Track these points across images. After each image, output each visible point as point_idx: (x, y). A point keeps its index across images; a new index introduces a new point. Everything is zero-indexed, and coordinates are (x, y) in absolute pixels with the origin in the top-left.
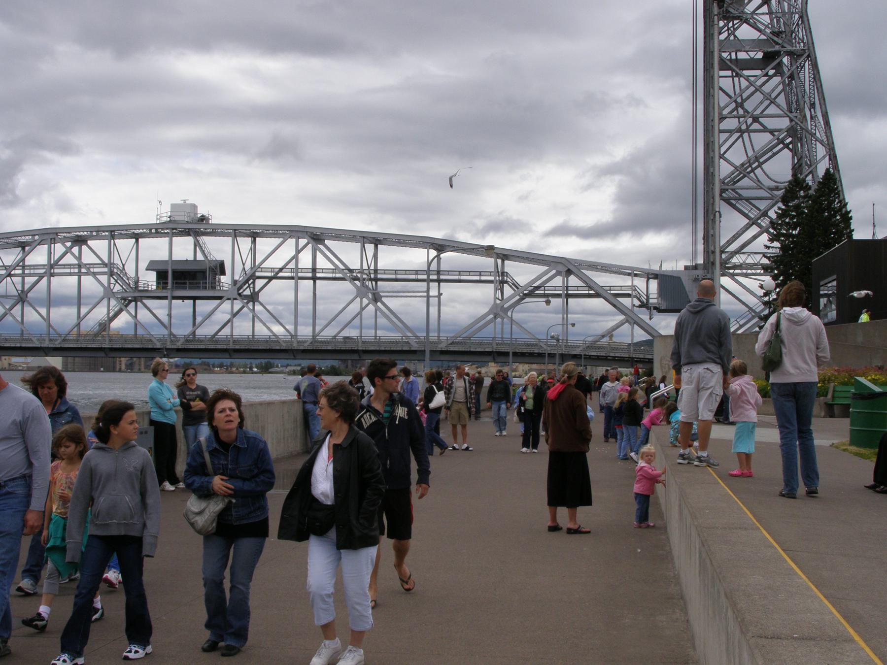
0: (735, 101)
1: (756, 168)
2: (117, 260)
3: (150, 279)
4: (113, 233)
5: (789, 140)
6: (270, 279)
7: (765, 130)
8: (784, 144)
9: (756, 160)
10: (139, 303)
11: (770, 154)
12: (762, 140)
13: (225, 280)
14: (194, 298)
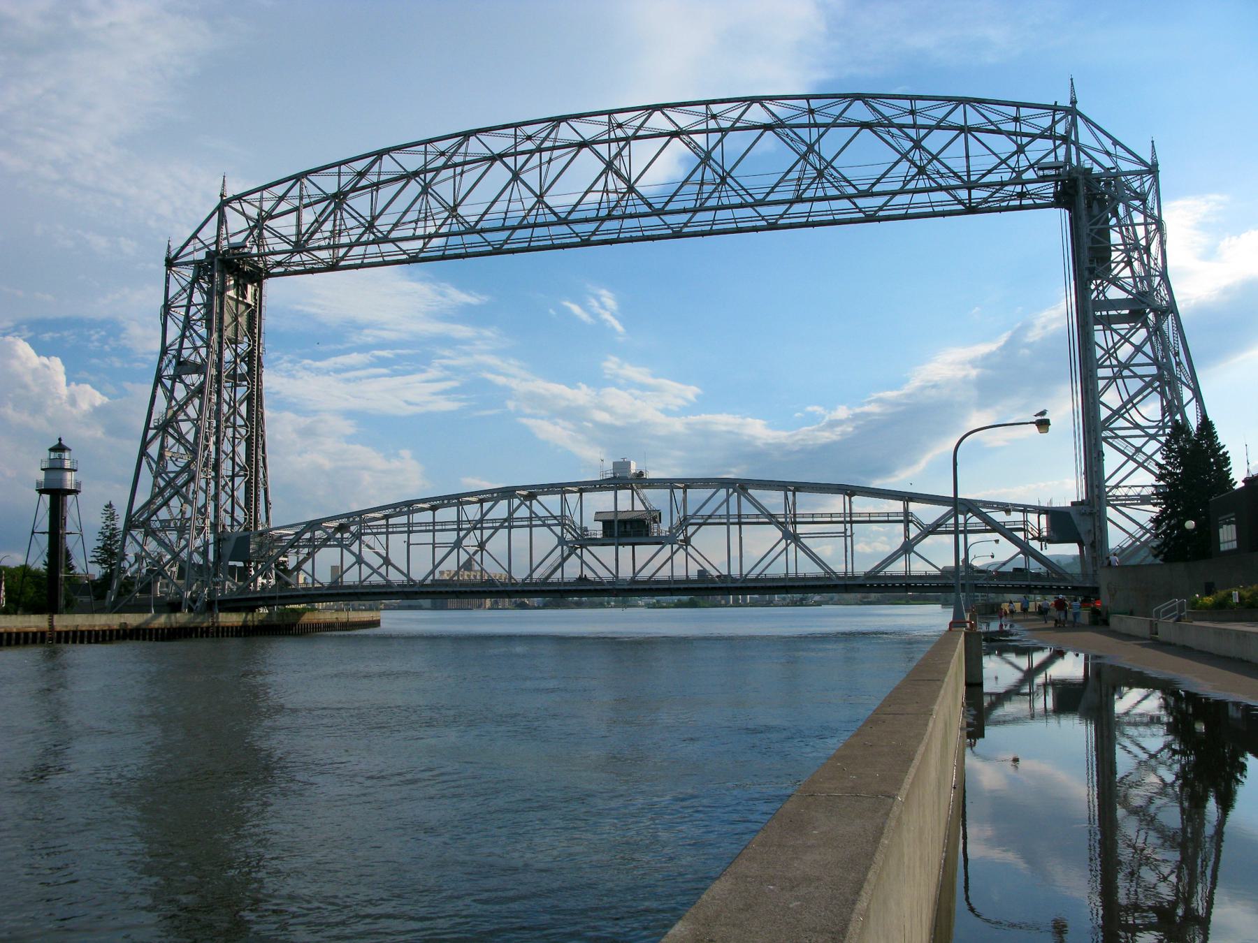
0: (1109, 353)
1: (1131, 408)
2: (567, 513)
3: (596, 529)
4: (560, 489)
5: (1157, 384)
6: (700, 525)
7: (1135, 376)
8: (1152, 387)
9: (1130, 402)
10: (584, 550)
11: (1140, 397)
12: (1134, 385)
13: (664, 527)
14: (633, 545)
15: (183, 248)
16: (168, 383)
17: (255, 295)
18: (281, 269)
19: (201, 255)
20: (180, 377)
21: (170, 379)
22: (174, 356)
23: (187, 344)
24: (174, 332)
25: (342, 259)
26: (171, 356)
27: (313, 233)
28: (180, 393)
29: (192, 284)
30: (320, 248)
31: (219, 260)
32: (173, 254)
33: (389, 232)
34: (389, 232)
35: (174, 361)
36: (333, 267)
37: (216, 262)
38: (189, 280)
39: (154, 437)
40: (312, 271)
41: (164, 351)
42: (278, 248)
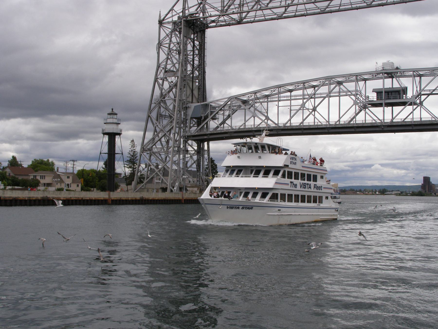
15: (167, 15)
16: (161, 81)
17: (202, 37)
18: (214, 24)
19: (175, 18)
20: (166, 78)
21: (161, 79)
22: (163, 68)
23: (169, 62)
24: (163, 56)
25: (245, 18)
26: (162, 68)
27: (229, 6)
28: (166, 85)
29: (172, 32)
30: (233, 13)
31: (184, 20)
32: (162, 18)
33: (268, 4)
34: (268, 4)
35: (163, 71)
36: (240, 22)
37: (182, 22)
38: (170, 30)
39: (155, 107)
40: (229, 25)
41: (158, 67)
42: (213, 14)
